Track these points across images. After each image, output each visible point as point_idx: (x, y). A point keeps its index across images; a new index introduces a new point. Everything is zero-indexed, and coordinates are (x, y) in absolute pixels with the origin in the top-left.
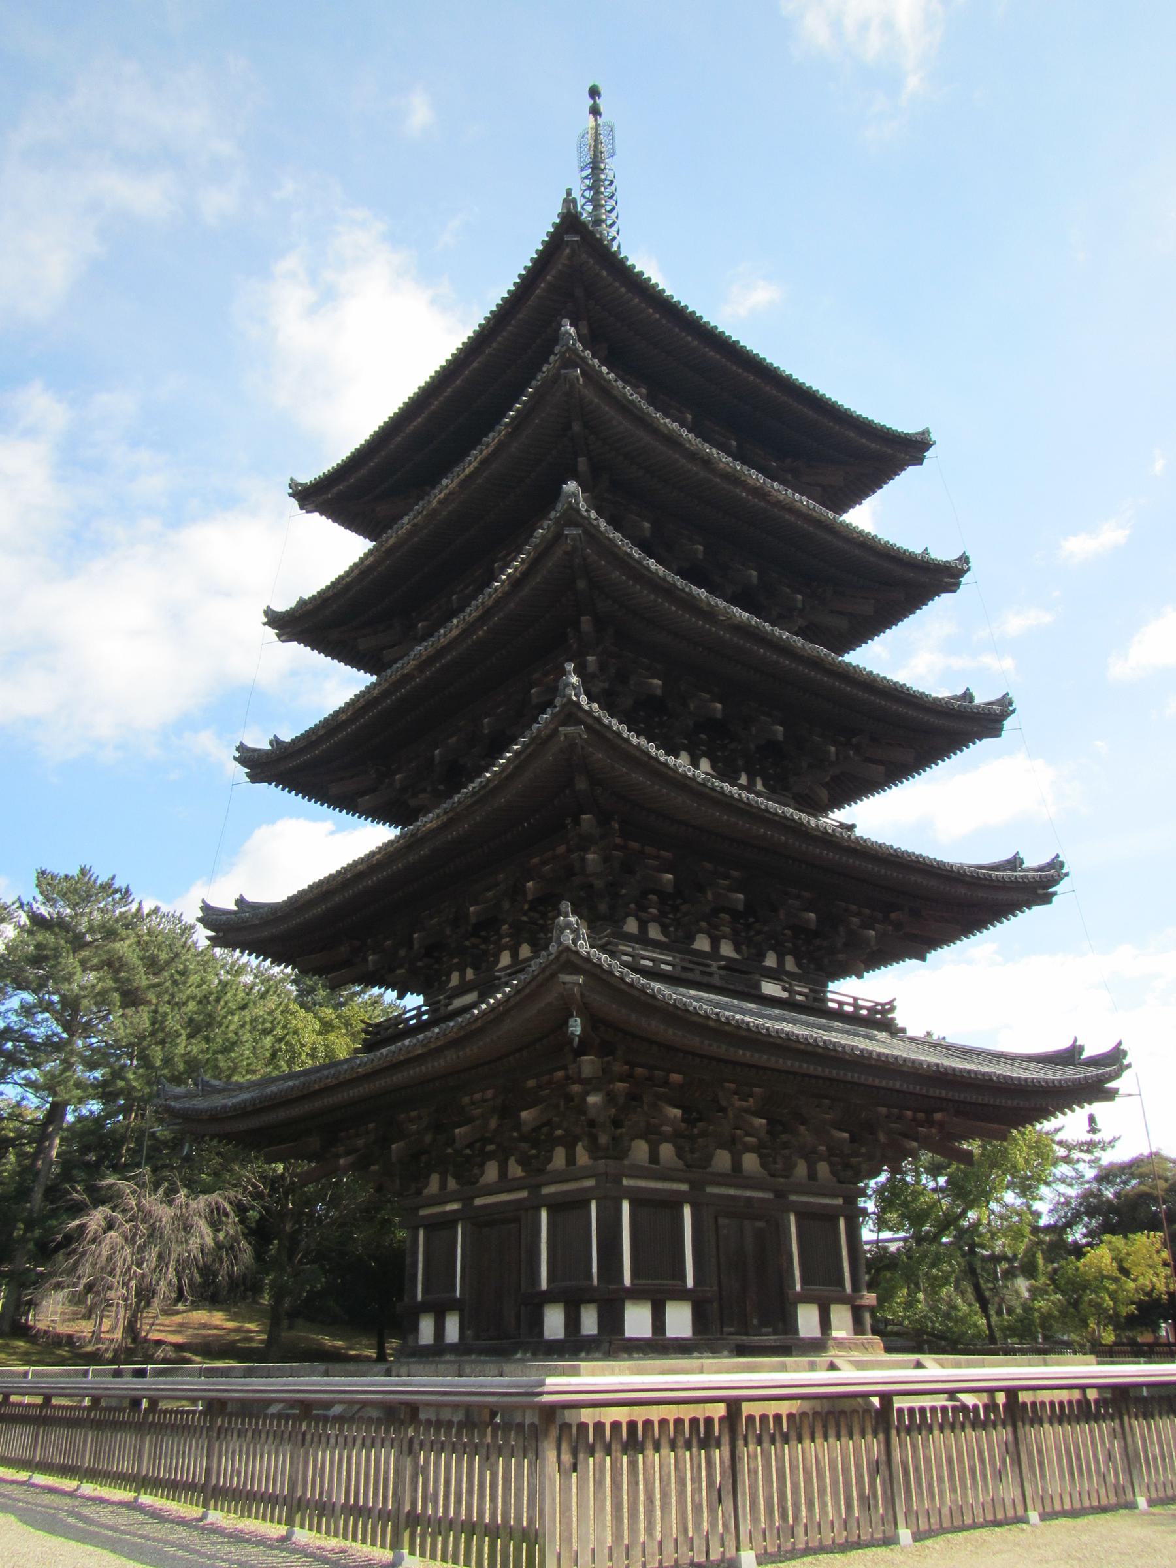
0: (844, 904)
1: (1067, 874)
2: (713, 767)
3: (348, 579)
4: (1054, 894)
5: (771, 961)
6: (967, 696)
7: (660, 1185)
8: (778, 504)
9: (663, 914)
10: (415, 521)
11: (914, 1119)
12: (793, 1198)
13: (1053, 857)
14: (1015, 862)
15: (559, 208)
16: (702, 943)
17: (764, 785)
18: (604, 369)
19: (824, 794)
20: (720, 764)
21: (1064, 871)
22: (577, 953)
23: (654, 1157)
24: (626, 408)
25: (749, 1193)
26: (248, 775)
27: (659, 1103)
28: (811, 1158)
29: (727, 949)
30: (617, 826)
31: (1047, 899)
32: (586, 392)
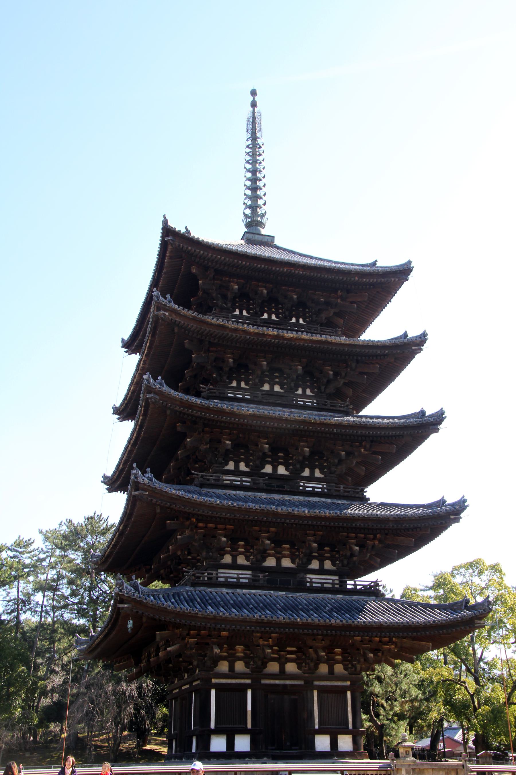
0: (346, 534)
1: (468, 506)
2: (286, 470)
3: (129, 396)
4: (461, 518)
5: (315, 565)
6: (422, 413)
7: (233, 681)
8: (291, 339)
9: (247, 551)
10: (139, 372)
11: (380, 641)
12: (316, 683)
13: (462, 496)
14: (442, 502)
15: (161, 226)
16: (271, 562)
17: (321, 473)
18: (176, 306)
19: (362, 471)
20: (291, 467)
21: (466, 504)
22: (123, 595)
23: (232, 668)
24: (194, 319)
25: (288, 682)
26: (107, 489)
27: (214, 646)
28: (331, 662)
29: (286, 563)
30: (195, 520)
31: (457, 520)
32: (170, 318)
